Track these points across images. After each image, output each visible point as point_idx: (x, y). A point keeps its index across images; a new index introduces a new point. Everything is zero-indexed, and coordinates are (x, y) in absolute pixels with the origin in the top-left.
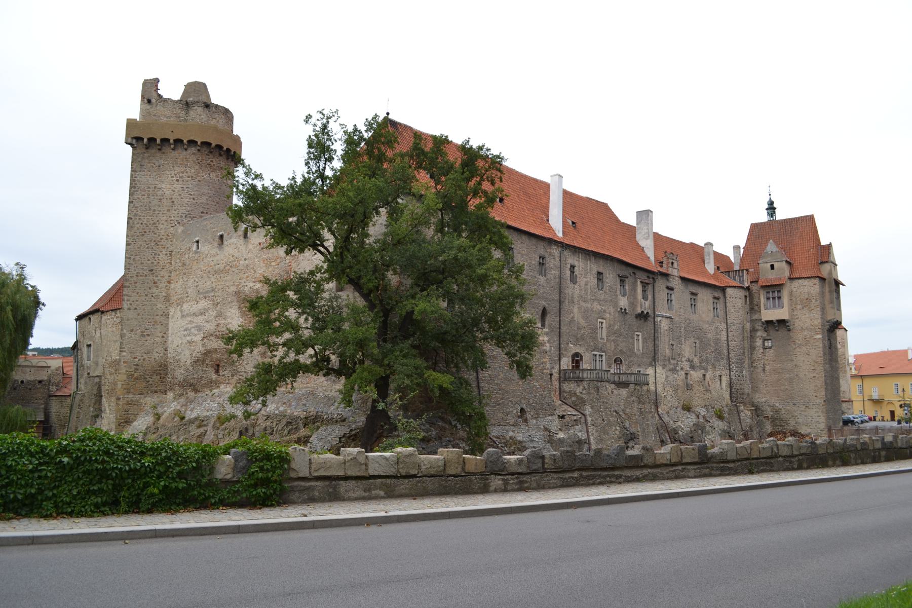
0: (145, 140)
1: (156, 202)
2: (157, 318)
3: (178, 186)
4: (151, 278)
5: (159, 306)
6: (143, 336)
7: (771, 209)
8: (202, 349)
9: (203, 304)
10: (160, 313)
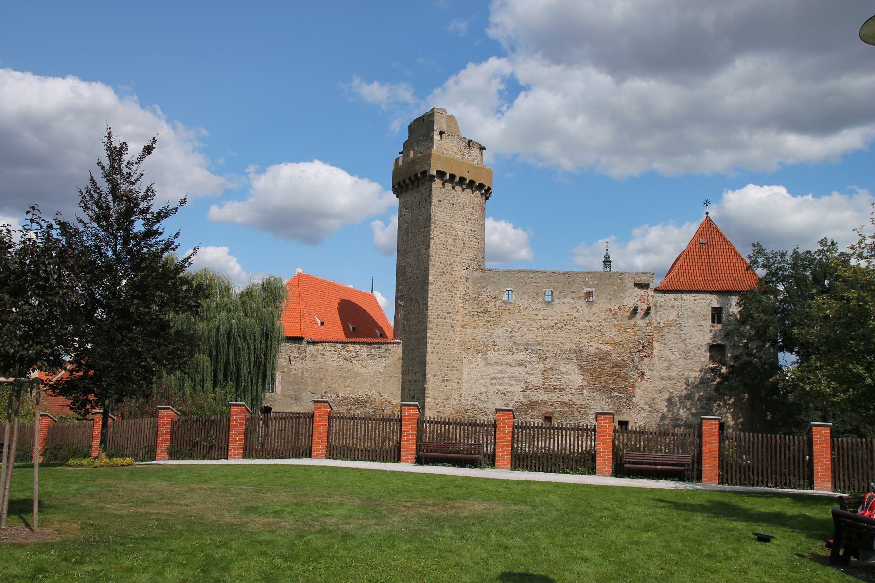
0: (448, 176)
1: (451, 242)
2: (454, 364)
3: (467, 228)
5: (455, 350)
6: (443, 381)
7: (607, 261)
8: (526, 401)
9: (520, 356)
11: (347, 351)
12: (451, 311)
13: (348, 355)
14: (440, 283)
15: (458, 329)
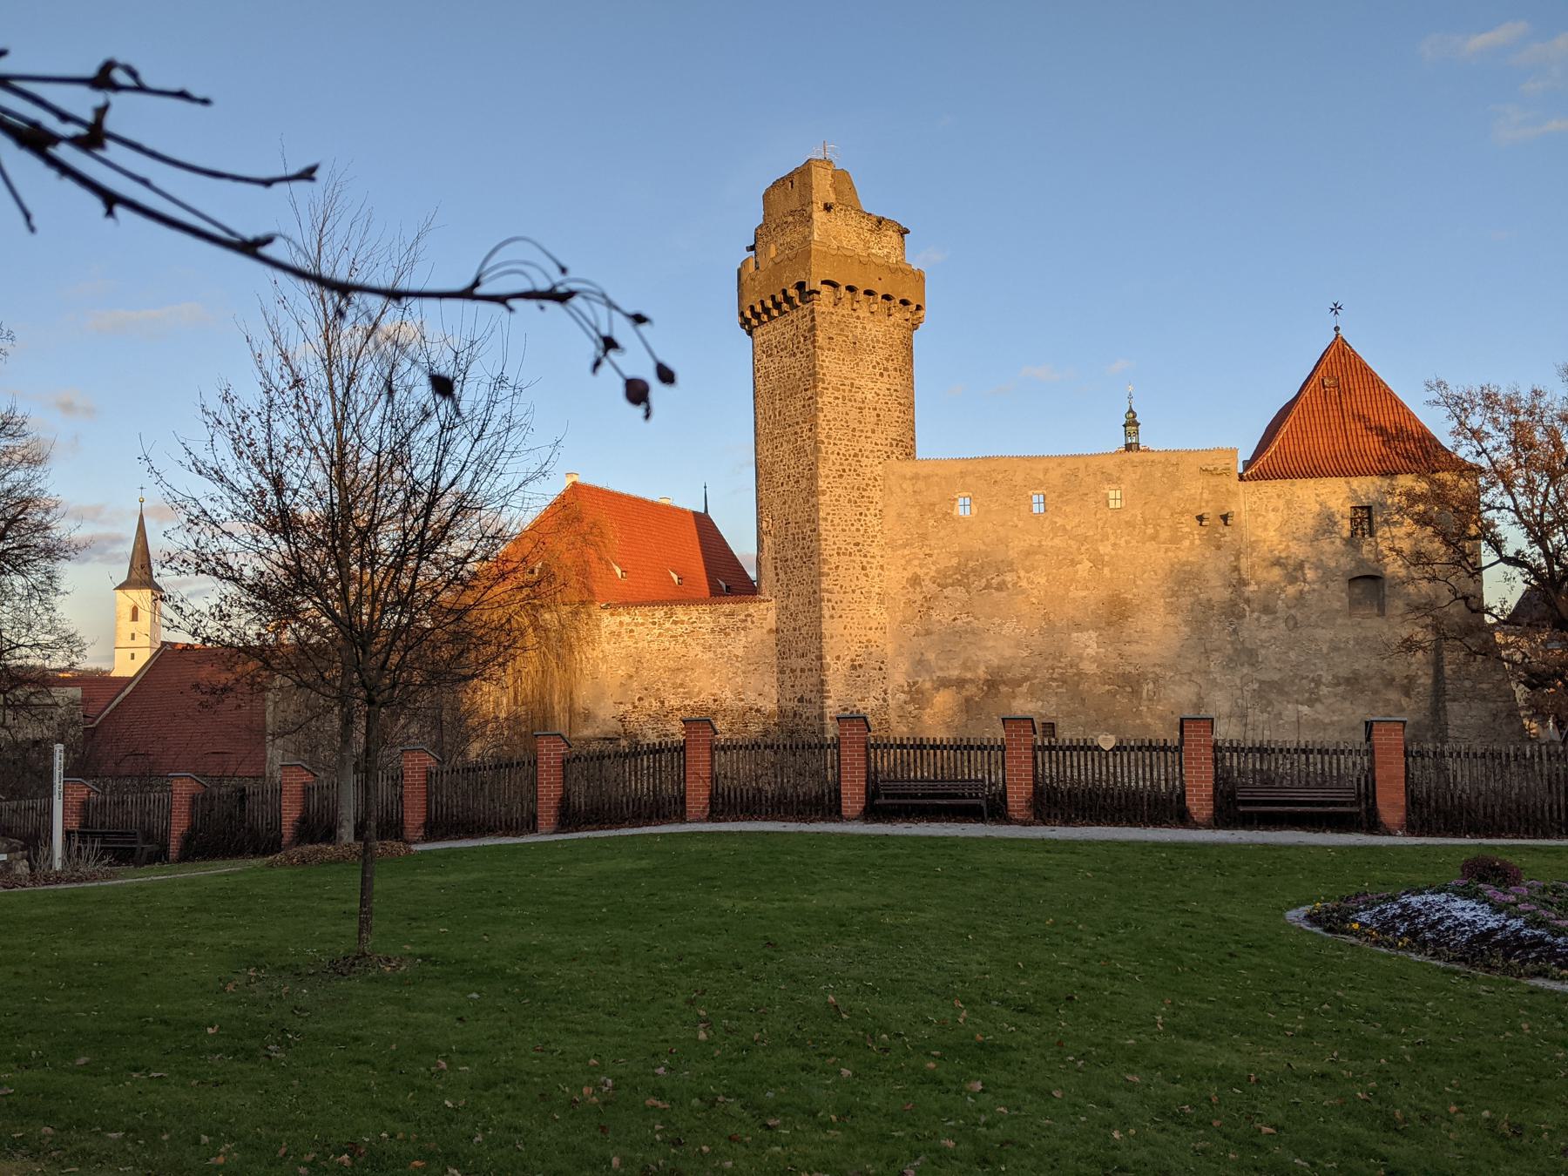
1: (854, 413)
3: (882, 385)
4: (858, 559)
10: (874, 625)
11: (675, 623)
12: (860, 540)
13: (679, 629)
14: (839, 491)
15: (873, 572)
